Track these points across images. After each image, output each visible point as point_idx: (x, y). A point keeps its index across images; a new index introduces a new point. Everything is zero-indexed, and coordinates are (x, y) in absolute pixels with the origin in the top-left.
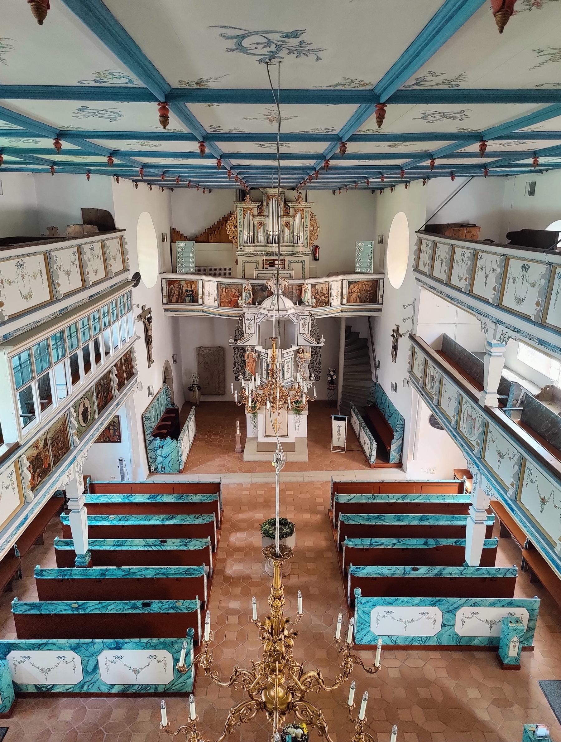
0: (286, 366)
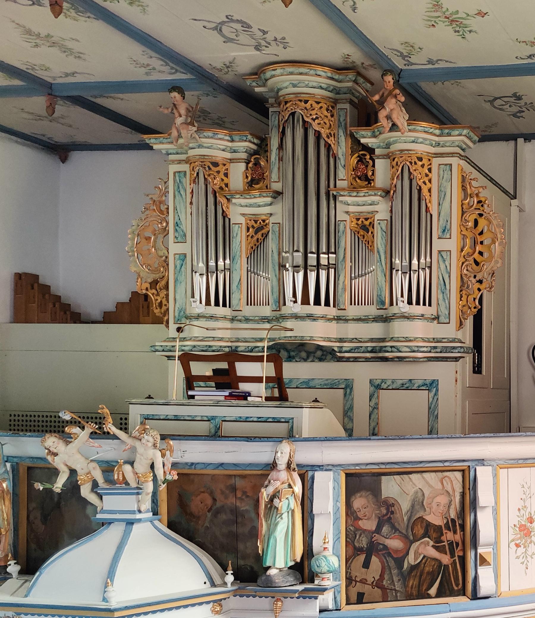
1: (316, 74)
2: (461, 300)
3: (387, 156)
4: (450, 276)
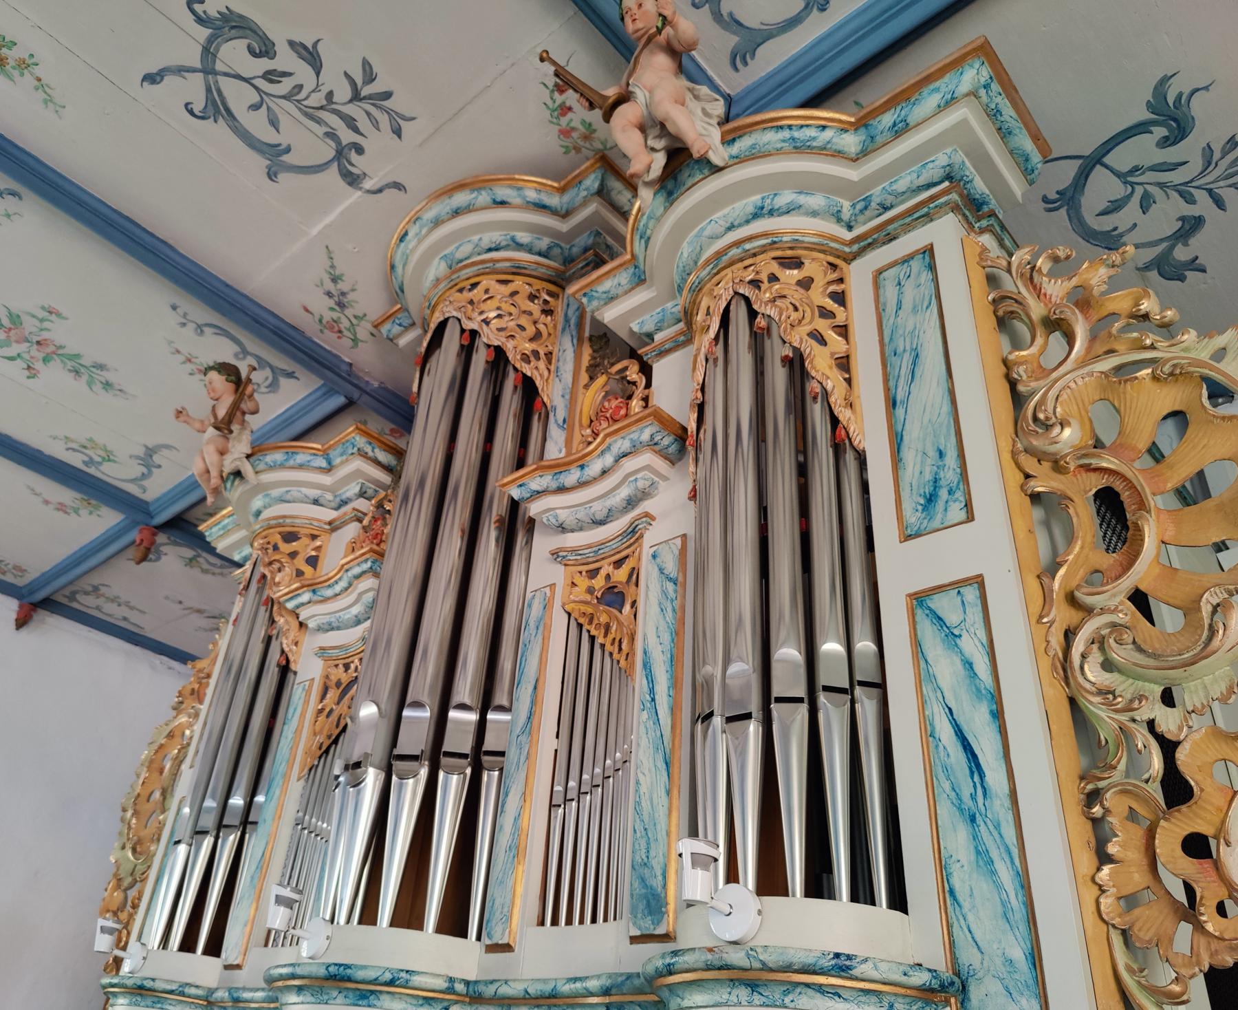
1: (495, 202)
2: (1104, 858)
4: (998, 715)
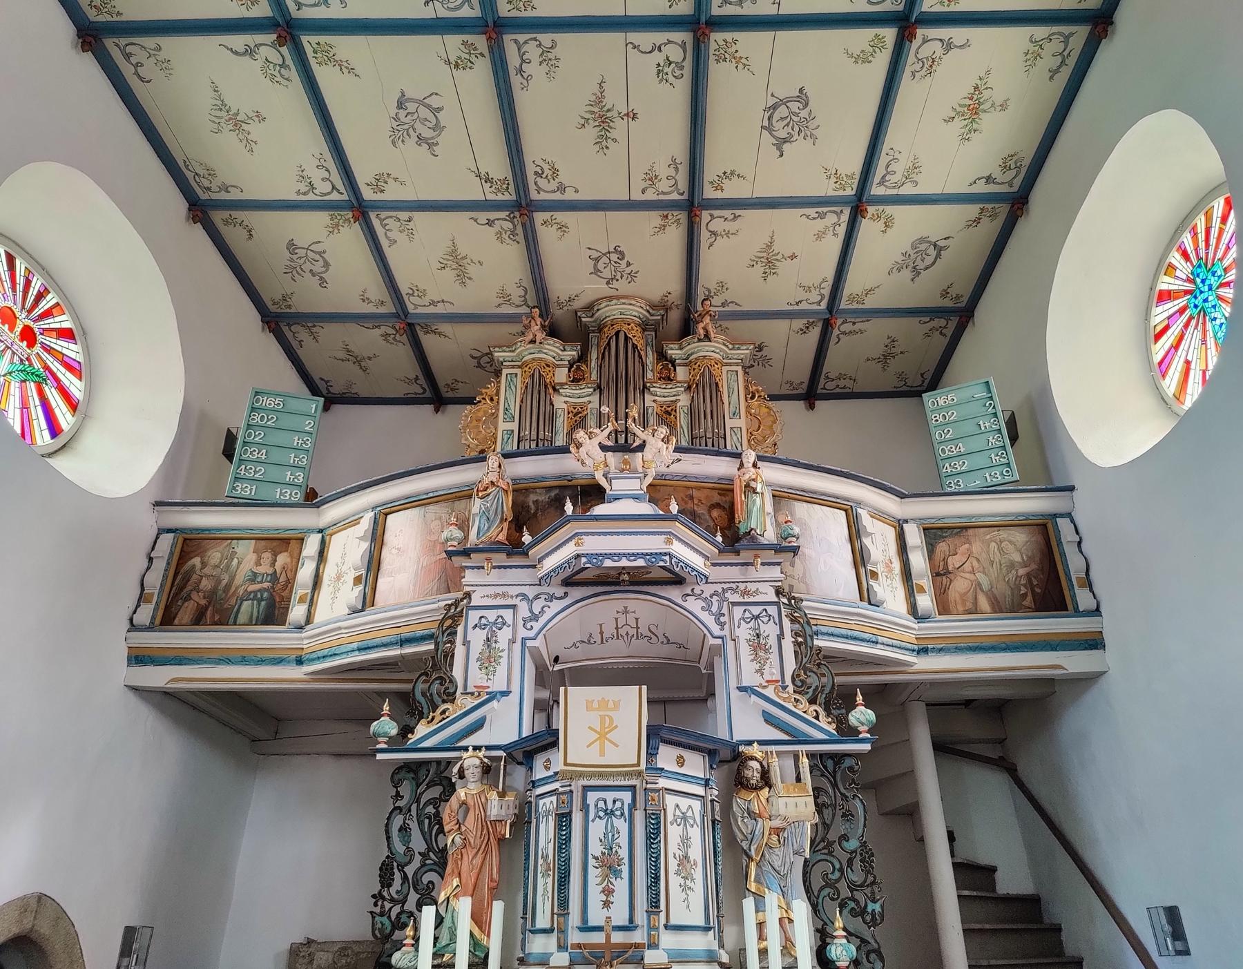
0: (674, 833)
3: (685, 365)
